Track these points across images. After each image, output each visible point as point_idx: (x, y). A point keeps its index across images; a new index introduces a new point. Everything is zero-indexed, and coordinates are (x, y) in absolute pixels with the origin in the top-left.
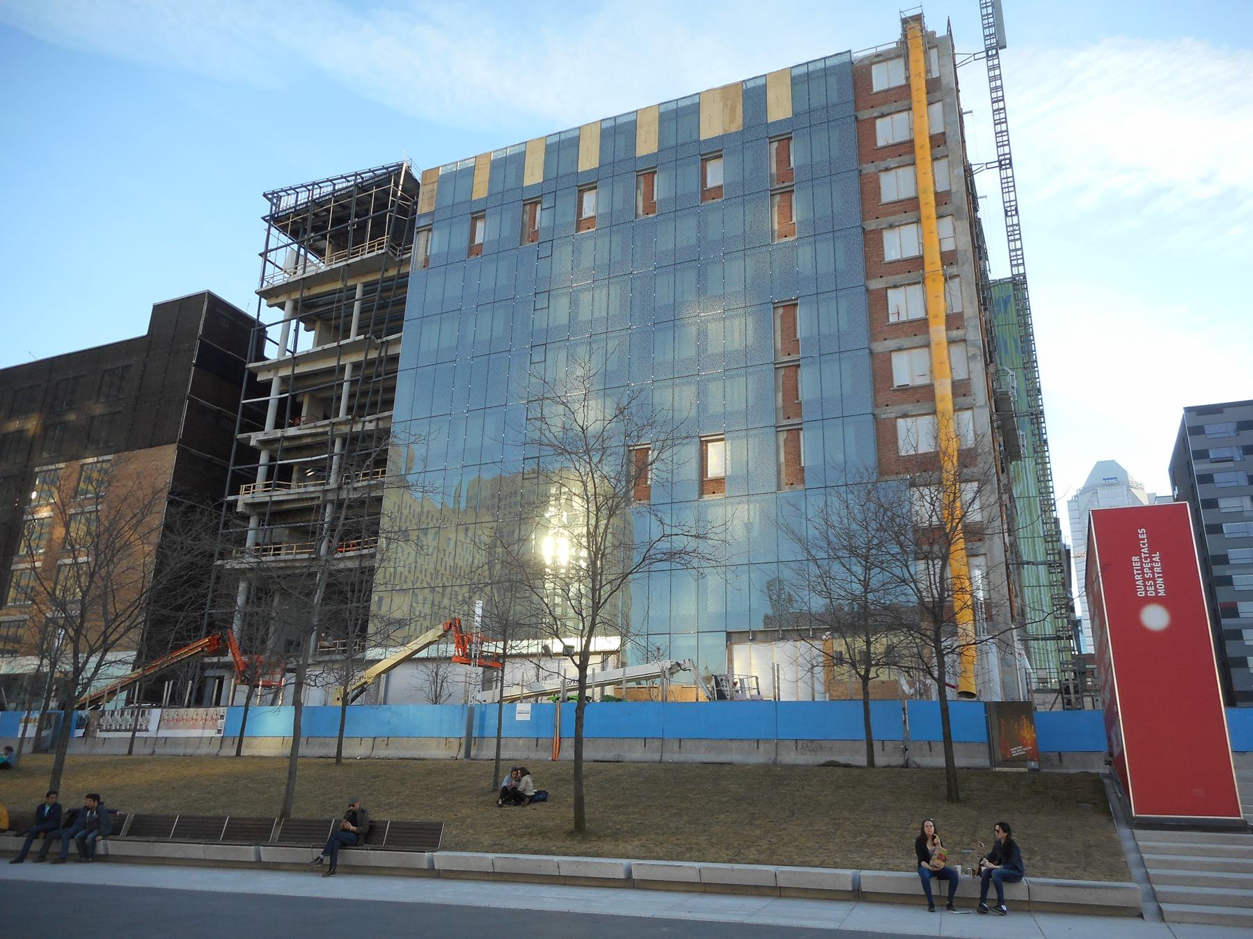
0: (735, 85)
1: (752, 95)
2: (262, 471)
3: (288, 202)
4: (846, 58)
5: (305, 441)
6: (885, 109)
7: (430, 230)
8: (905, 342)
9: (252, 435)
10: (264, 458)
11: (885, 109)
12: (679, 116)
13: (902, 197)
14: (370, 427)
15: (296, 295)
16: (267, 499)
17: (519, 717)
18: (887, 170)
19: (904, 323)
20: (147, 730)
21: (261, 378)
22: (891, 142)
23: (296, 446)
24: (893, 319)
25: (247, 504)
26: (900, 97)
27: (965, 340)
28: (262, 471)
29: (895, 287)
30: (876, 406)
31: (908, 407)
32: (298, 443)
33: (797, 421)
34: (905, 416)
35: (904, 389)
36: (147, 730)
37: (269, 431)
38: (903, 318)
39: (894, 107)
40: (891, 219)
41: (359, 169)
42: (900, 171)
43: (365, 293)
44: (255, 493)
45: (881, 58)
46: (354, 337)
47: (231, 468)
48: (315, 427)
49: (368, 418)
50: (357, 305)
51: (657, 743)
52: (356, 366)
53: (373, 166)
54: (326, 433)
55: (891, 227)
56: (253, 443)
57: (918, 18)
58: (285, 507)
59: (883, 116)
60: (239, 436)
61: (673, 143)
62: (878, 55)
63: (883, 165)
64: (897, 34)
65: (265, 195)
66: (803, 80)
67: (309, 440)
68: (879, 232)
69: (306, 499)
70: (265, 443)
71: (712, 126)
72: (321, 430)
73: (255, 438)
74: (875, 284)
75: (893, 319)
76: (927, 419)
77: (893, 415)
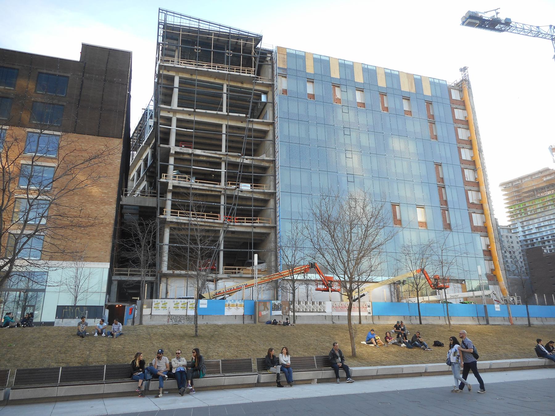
0: (411, 74)
1: (418, 82)
3: (171, 20)
4: (444, 83)
5: (201, 158)
6: (457, 106)
7: (283, 77)
12: (393, 77)
15: (181, 75)
16: (189, 186)
17: (497, 310)
20: (324, 312)
33: (445, 207)
34: (474, 213)
35: (473, 203)
36: (324, 312)
39: (459, 107)
49: (246, 157)
50: (225, 96)
51: (540, 319)
52: (229, 127)
60: (161, 145)
65: (160, 9)
66: (434, 84)
67: (205, 159)
71: (406, 87)
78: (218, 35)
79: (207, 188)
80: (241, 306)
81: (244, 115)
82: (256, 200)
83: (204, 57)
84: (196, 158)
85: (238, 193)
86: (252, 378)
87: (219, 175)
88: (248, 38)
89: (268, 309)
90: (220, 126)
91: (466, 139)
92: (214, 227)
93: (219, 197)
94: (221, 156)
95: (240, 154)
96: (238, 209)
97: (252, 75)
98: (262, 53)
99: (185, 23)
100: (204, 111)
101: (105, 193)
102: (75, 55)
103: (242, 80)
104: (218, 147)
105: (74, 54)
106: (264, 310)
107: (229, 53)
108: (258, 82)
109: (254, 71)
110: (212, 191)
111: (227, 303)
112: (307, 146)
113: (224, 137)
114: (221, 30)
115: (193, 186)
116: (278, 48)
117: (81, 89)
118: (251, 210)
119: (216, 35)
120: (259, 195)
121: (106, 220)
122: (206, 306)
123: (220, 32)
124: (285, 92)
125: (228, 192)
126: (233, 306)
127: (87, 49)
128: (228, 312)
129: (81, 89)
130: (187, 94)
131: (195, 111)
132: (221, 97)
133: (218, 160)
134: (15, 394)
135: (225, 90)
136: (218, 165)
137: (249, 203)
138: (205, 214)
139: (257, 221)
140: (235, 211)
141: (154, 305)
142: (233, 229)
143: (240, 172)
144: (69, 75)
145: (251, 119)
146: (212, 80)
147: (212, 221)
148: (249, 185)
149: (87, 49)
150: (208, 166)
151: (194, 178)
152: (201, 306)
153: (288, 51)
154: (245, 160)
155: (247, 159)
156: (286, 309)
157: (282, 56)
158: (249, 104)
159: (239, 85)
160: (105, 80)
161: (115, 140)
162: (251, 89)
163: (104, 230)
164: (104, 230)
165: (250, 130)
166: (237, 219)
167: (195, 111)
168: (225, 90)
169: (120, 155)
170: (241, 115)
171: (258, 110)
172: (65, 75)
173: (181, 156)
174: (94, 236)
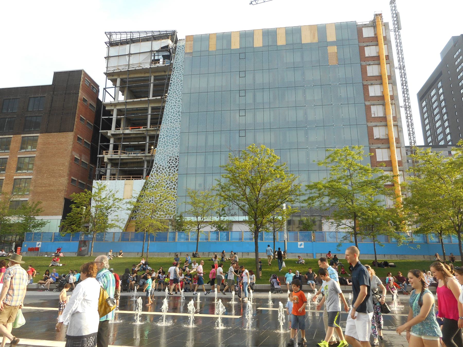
2: (111, 146)
5: (132, 136)
6: (368, 44)
8: (378, 124)
9: (109, 131)
10: (112, 141)
11: (368, 44)
13: (374, 75)
16: (119, 157)
18: (369, 65)
19: (377, 117)
21: (107, 108)
22: (370, 56)
23: (127, 137)
24: (373, 116)
25: (108, 159)
26: (374, 40)
27: (397, 126)
28: (111, 146)
29: (374, 105)
30: (369, 144)
31: (379, 145)
32: (128, 136)
34: (379, 148)
35: (378, 139)
37: (113, 130)
38: (376, 116)
39: (371, 44)
40: (372, 82)
41: (153, 30)
42: (373, 66)
43: (155, 80)
44: (108, 156)
45: (366, 26)
46: (151, 98)
47: (99, 144)
50: (152, 85)
53: (161, 29)
54: (144, 133)
55: (372, 84)
56: (109, 134)
57: (380, 15)
58: (125, 161)
59: (367, 46)
61: (291, 42)
62: (365, 25)
63: (368, 63)
64: (372, 18)
65: (105, 33)
66: (340, 27)
67: (134, 136)
68: (367, 86)
69: (138, 159)
70: (113, 135)
71: (307, 39)
72: (141, 132)
73: (109, 133)
74: (368, 103)
75: (373, 116)
76: (386, 150)
77: (375, 147)
79: (132, 157)
81: (160, 97)
87: (144, 145)
89: (86, 246)
90: (146, 109)
91: (378, 75)
93: (143, 162)
102: (49, 81)
104: (145, 124)
105: (49, 81)
110: (135, 159)
114: (148, 35)
115: (121, 157)
121: (61, 188)
125: (148, 158)
127: (57, 75)
132: (148, 86)
136: (144, 138)
144: (45, 95)
146: (143, 75)
149: (57, 75)
159: (163, 74)
160: (65, 94)
161: (69, 133)
162: (164, 76)
164: (60, 194)
172: (44, 95)
173: (118, 137)
174: (54, 199)
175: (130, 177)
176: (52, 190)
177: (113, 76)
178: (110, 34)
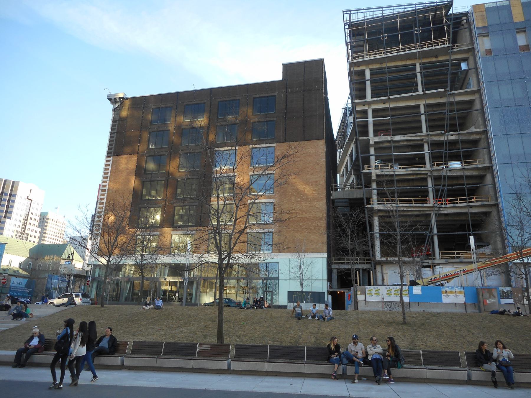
3: (355, 18)
7: (484, 36)
14: (451, 138)
15: (371, 67)
16: (392, 173)
48: (416, 136)
49: (451, 133)
50: (419, 75)
52: (427, 106)
60: (360, 138)
65: (343, 11)
67: (405, 143)
72: (418, 138)
78: (404, 15)
79: (412, 172)
80: (460, 293)
81: (443, 90)
82: (468, 177)
83: (392, 42)
84: (397, 144)
85: (446, 173)
86: (462, 375)
87: (422, 157)
88: (436, 8)
90: (418, 107)
92: (423, 211)
93: (425, 180)
94: (423, 138)
95: (443, 132)
96: (448, 190)
97: (446, 46)
98: (457, 19)
99: (369, 15)
100: (398, 96)
101: (316, 190)
102: (277, 75)
103: (435, 53)
104: (419, 129)
105: (277, 75)
106: (490, 298)
107: (417, 30)
108: (455, 50)
109: (449, 41)
110: (417, 174)
111: (444, 290)
112: (527, 106)
113: (423, 117)
114: (406, 10)
115: (396, 173)
116: (474, 7)
117: (286, 103)
118: (463, 190)
119: (401, 16)
120: (471, 172)
121: (319, 215)
122: (420, 293)
123: (405, 12)
124: (489, 52)
125: (435, 174)
126: (451, 292)
127: (288, 68)
128: (445, 299)
129: (286, 103)
130: (380, 84)
131: (389, 99)
132: (415, 77)
133: (419, 142)
134: (236, 365)
135: (418, 69)
137: (461, 182)
138: (413, 199)
139: (473, 200)
140: (445, 193)
141: (367, 292)
142: (446, 212)
143: (446, 150)
144: (276, 94)
145: (452, 92)
146: (403, 63)
147: (420, 205)
148: (459, 163)
149: (288, 68)
150: (409, 150)
151: (398, 164)
152: (415, 293)
153: (486, 6)
154: (449, 136)
155: (452, 135)
156: (518, 297)
157: (481, 14)
158: (445, 76)
159: (434, 59)
160: (304, 91)
162: (448, 61)
163: (319, 224)
164: (319, 224)
165: (452, 104)
166: (449, 201)
167: (389, 99)
168: (418, 69)
169: (325, 154)
170: (439, 90)
171: (458, 80)
172: (273, 94)
173: (381, 145)
174: (311, 229)
175: (411, 200)
176: (306, 218)
177: (359, 66)
178: (349, 12)
